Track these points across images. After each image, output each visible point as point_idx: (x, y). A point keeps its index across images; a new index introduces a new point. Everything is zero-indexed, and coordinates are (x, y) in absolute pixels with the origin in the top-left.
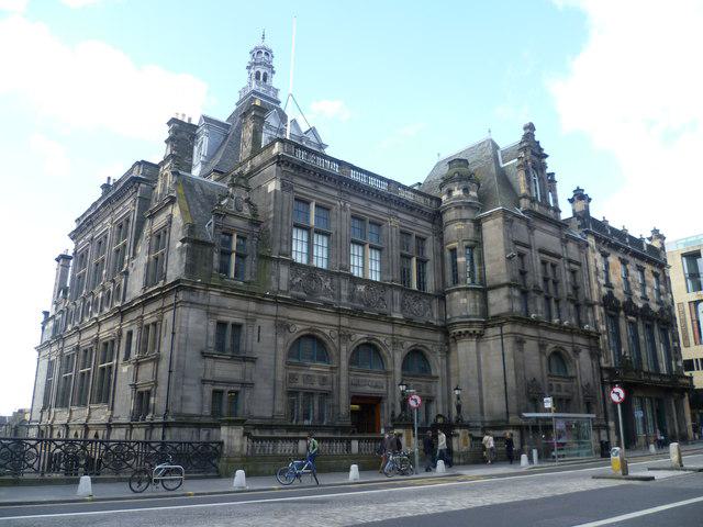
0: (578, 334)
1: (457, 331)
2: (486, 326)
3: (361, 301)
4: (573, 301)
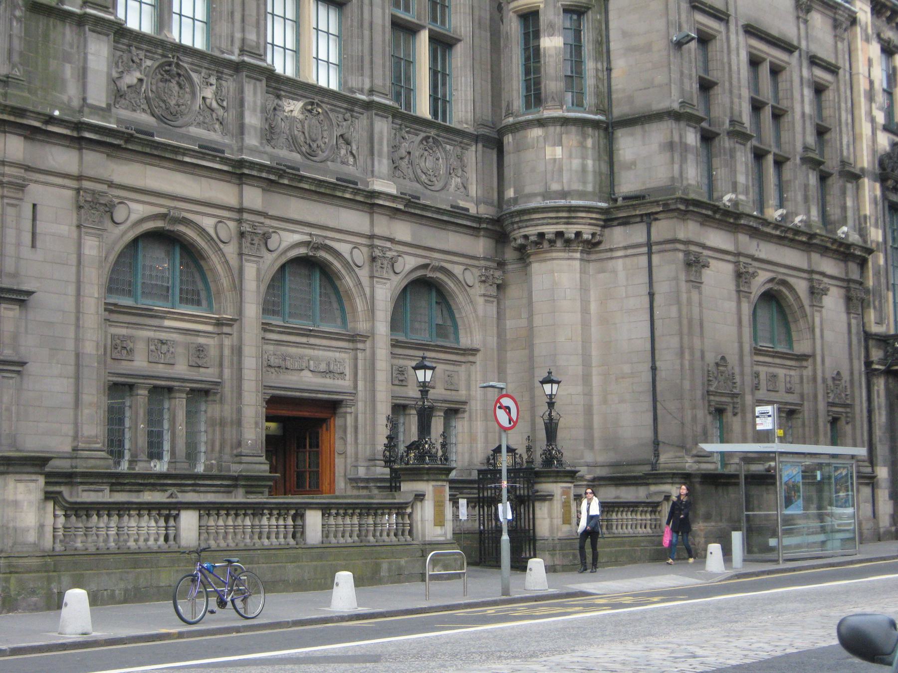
0: (824, 250)
1: (532, 231)
2: (609, 220)
3: (293, 144)
4: (814, 163)
